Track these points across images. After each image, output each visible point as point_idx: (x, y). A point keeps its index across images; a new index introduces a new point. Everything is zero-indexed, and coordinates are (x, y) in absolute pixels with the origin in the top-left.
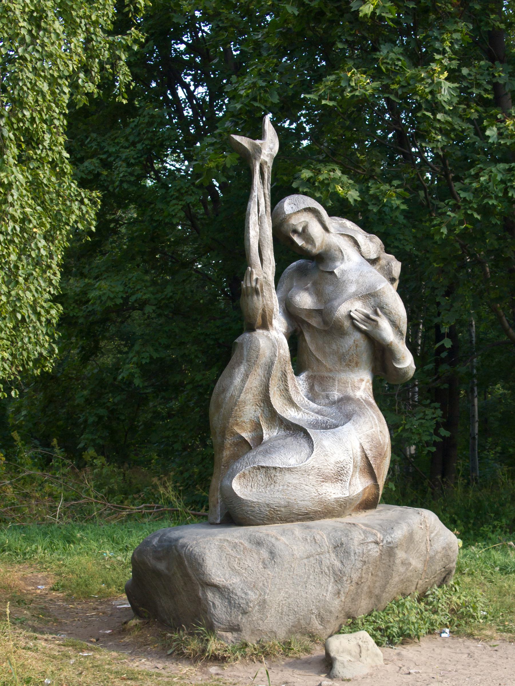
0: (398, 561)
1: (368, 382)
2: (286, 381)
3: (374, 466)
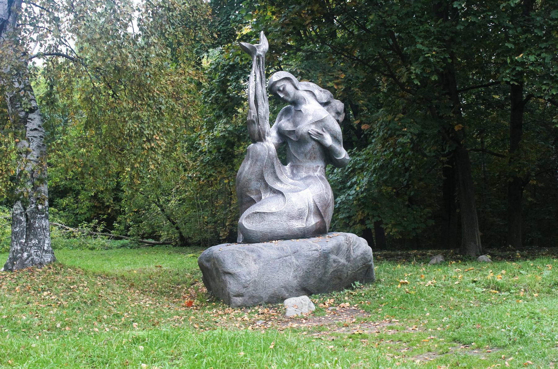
0: (331, 260)
1: (322, 167)
2: (274, 168)
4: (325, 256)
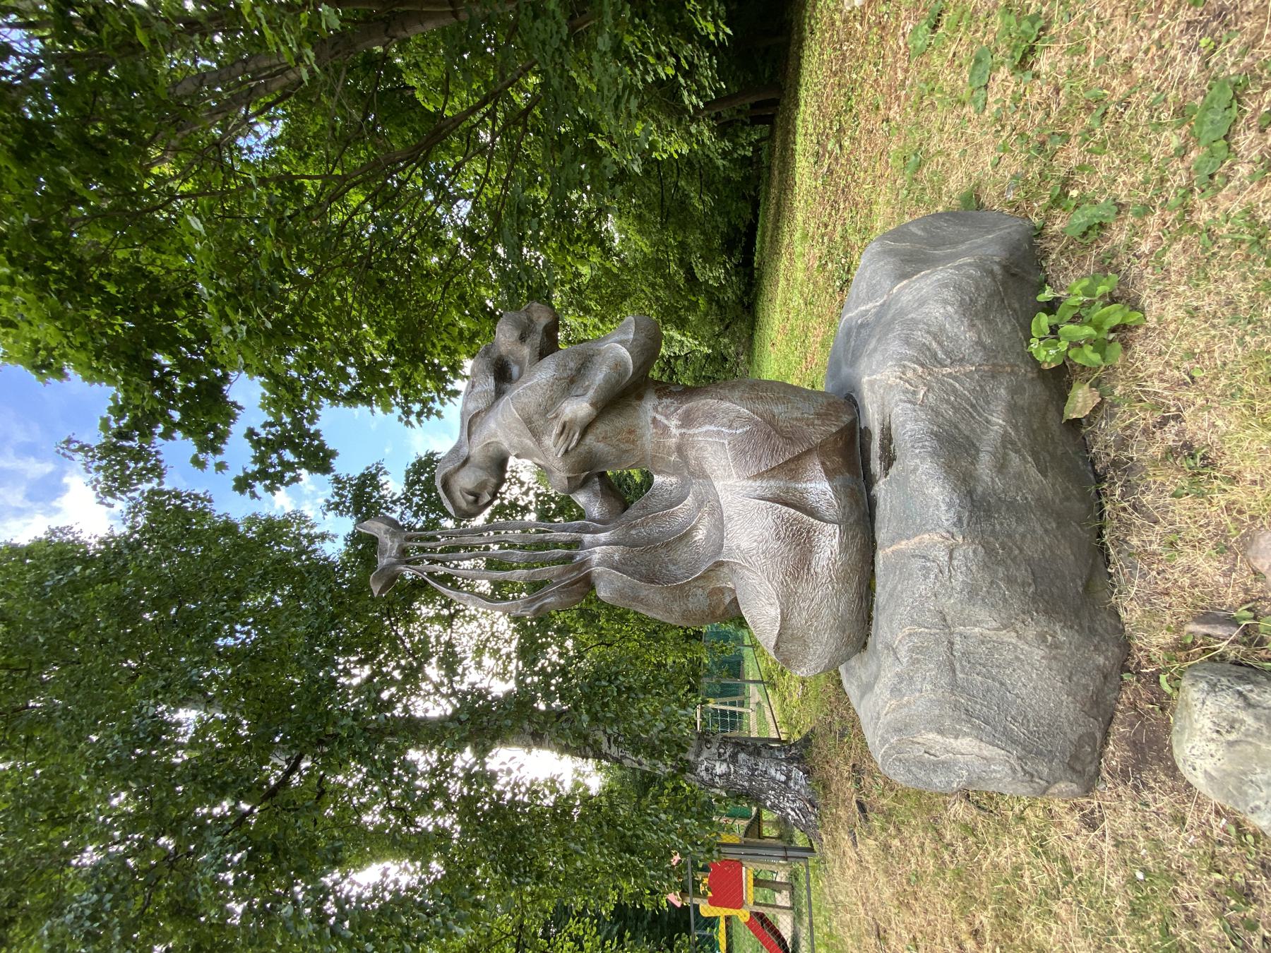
1: (655, 409)
3: (788, 456)
4: (977, 508)
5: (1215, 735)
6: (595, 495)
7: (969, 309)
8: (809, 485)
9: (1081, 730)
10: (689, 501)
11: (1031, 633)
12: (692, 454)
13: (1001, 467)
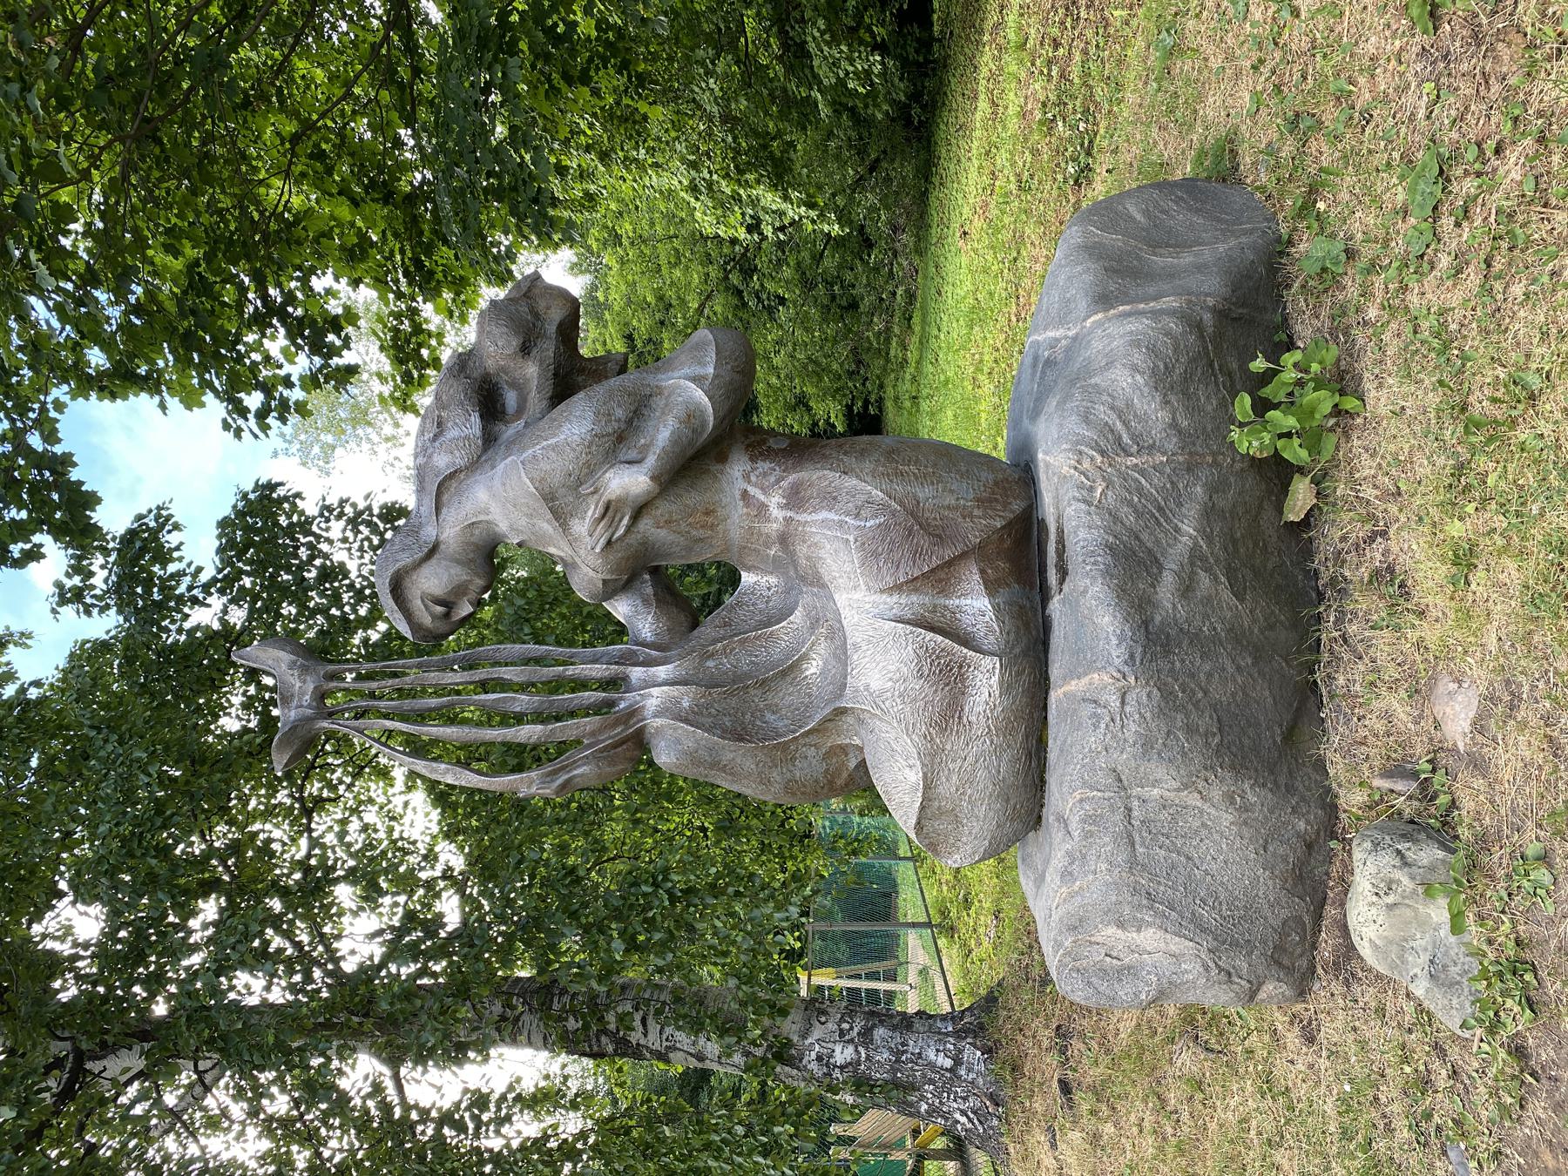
1: (746, 477)
3: (935, 562)
4: (1153, 641)
5: (1375, 898)
6: (646, 602)
7: (1166, 381)
8: (963, 602)
9: (1285, 913)
10: (797, 617)
11: (1216, 793)
12: (802, 550)
13: (1186, 589)
